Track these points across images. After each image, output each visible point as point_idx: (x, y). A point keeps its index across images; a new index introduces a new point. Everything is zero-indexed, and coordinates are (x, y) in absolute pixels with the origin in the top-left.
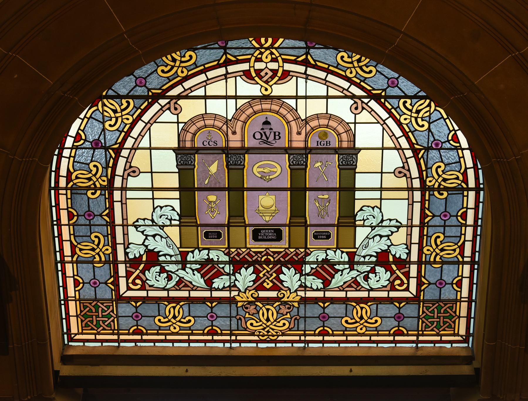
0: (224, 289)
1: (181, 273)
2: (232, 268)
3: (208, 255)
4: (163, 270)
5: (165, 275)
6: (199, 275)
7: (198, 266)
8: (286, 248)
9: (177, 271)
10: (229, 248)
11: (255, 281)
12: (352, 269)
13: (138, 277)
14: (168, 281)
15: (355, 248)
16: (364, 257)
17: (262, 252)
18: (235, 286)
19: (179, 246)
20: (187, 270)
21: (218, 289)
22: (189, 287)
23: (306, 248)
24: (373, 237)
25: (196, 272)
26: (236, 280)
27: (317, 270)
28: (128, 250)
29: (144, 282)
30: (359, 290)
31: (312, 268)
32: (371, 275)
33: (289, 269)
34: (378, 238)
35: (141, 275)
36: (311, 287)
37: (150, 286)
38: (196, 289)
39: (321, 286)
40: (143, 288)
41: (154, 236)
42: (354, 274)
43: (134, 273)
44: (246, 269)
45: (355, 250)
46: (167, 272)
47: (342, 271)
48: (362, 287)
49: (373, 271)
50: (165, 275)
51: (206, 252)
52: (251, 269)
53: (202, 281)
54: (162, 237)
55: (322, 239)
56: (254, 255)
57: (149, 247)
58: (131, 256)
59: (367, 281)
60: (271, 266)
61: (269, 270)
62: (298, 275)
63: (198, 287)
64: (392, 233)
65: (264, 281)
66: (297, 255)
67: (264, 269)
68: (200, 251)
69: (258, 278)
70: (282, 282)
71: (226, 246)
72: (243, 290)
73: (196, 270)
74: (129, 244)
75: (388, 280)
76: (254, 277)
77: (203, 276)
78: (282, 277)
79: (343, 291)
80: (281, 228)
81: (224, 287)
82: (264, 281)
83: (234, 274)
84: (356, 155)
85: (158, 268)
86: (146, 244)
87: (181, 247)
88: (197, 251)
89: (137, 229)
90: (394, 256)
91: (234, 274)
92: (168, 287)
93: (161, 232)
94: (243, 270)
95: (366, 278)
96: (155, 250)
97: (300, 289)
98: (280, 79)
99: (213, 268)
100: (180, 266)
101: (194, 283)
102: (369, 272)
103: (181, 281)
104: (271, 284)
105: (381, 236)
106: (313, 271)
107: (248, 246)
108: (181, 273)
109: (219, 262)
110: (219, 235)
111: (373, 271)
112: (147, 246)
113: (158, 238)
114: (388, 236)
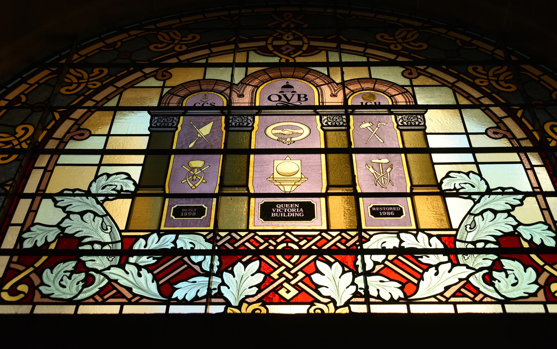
0: (195, 301)
1: (116, 273)
2: (217, 263)
3: (174, 242)
4: (81, 267)
5: (83, 276)
6: (150, 276)
7: (151, 261)
8: (322, 231)
9: (108, 268)
10: (216, 230)
11: (260, 287)
12: (455, 264)
13: (26, 280)
14: (84, 287)
15: (451, 229)
16: (474, 243)
17: (279, 237)
18: (220, 295)
19: (122, 227)
20: (128, 267)
21: (184, 302)
22: (123, 296)
23: (359, 229)
24: (481, 213)
25: (144, 272)
26: (223, 283)
27: (386, 266)
28: (25, 235)
29: (33, 288)
30: (481, 302)
31: (376, 263)
32: (495, 274)
33: (330, 264)
34: (489, 215)
35: (34, 277)
36: (379, 297)
37: (43, 296)
38: (139, 300)
39: (398, 294)
40: (28, 300)
41: (82, 214)
42: (461, 272)
43: (20, 272)
44: (246, 264)
45: (454, 233)
46: (87, 270)
47: (437, 266)
48: (486, 296)
49: (497, 266)
50: (83, 276)
51: (173, 237)
52: (255, 265)
53: (153, 287)
54: (96, 214)
55: (386, 216)
56: (262, 241)
57: (67, 231)
58: (27, 245)
59: (493, 285)
60: (296, 258)
61: (291, 266)
62: (350, 275)
63: (142, 297)
64: (513, 207)
65: (281, 286)
66: (344, 241)
67: (280, 264)
68: (160, 236)
69: (268, 280)
70: (316, 287)
71: (211, 227)
72: (234, 303)
73: (146, 267)
74: (33, 224)
75: (536, 282)
76: (260, 278)
77: (156, 278)
78: (316, 278)
79: (447, 302)
80: (313, 200)
81: (196, 298)
82: (281, 286)
83: (219, 274)
84: (423, 115)
85: (71, 265)
86: (63, 225)
87: (126, 230)
88: (155, 236)
89: (56, 202)
90: (531, 242)
91: (219, 274)
92: (81, 297)
93: (99, 209)
94: (239, 267)
95: (489, 280)
96: (77, 235)
97: (354, 300)
98: (305, 52)
99: (181, 262)
100: (116, 260)
101: (135, 291)
102: (491, 269)
103: (111, 284)
104: (294, 292)
105: (495, 212)
106: (378, 268)
107: (251, 227)
108: (116, 273)
109: (194, 252)
110: (200, 212)
111: (497, 266)
112: (63, 229)
113: (88, 217)
114: (508, 212)
